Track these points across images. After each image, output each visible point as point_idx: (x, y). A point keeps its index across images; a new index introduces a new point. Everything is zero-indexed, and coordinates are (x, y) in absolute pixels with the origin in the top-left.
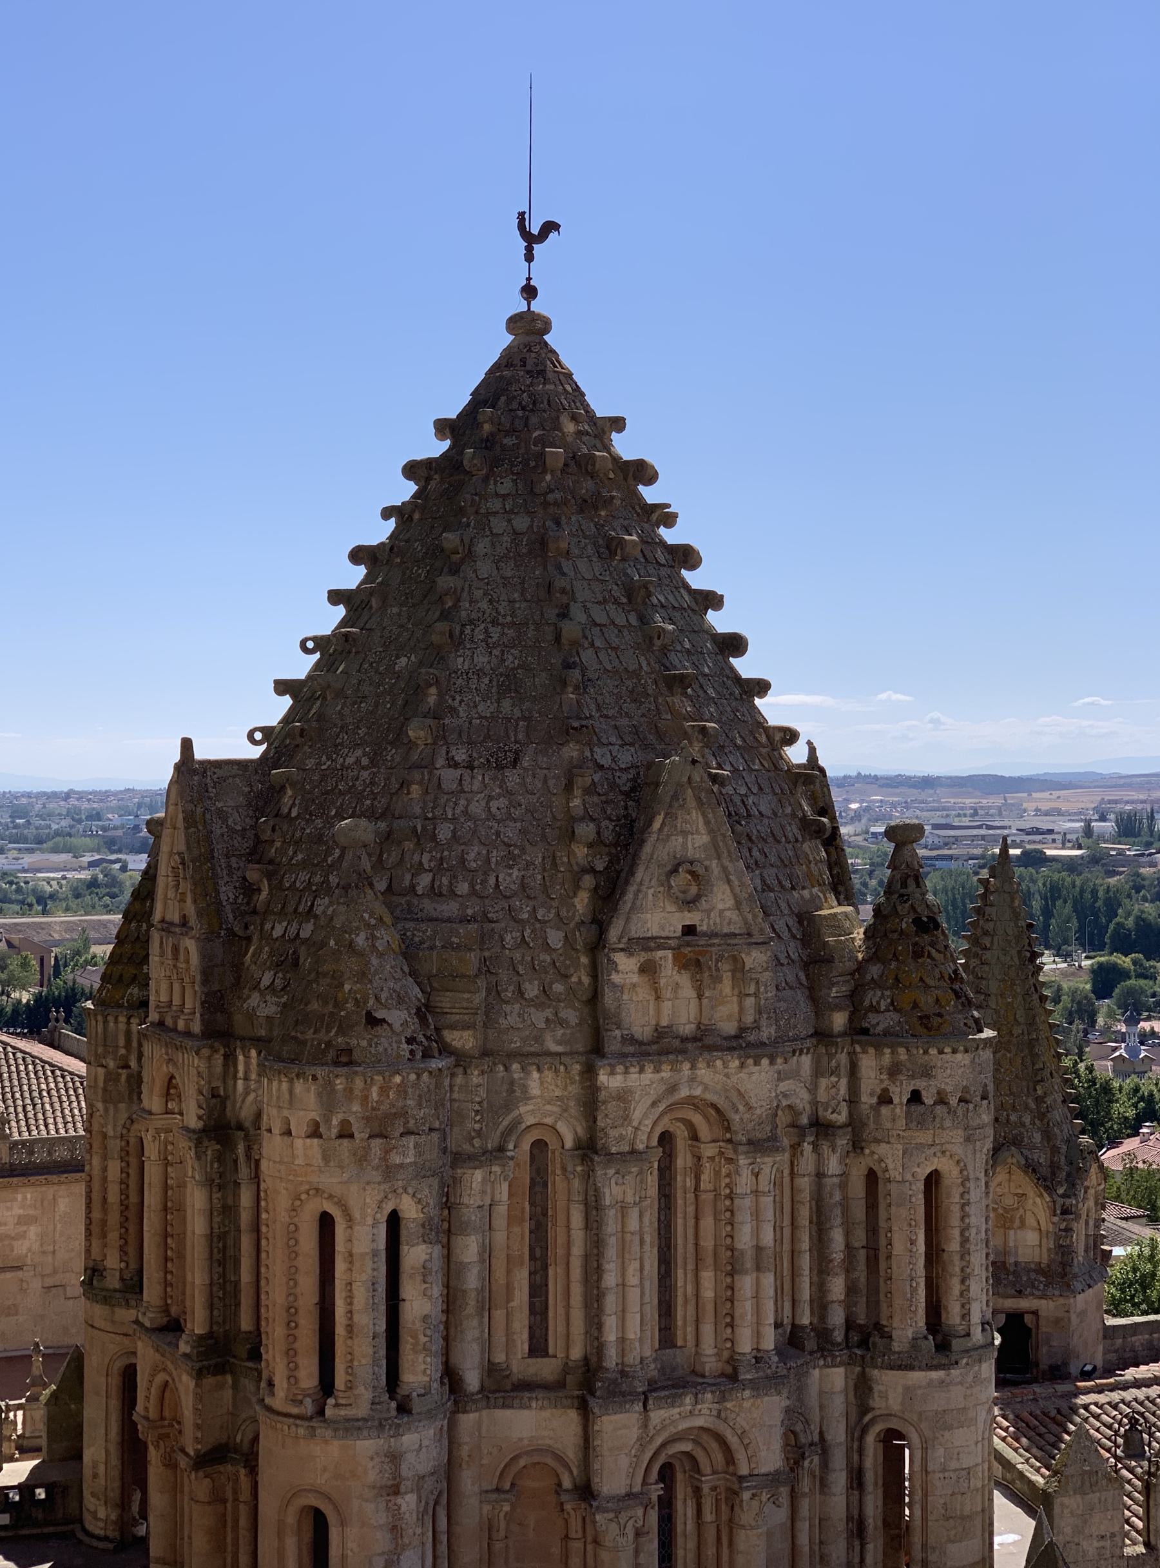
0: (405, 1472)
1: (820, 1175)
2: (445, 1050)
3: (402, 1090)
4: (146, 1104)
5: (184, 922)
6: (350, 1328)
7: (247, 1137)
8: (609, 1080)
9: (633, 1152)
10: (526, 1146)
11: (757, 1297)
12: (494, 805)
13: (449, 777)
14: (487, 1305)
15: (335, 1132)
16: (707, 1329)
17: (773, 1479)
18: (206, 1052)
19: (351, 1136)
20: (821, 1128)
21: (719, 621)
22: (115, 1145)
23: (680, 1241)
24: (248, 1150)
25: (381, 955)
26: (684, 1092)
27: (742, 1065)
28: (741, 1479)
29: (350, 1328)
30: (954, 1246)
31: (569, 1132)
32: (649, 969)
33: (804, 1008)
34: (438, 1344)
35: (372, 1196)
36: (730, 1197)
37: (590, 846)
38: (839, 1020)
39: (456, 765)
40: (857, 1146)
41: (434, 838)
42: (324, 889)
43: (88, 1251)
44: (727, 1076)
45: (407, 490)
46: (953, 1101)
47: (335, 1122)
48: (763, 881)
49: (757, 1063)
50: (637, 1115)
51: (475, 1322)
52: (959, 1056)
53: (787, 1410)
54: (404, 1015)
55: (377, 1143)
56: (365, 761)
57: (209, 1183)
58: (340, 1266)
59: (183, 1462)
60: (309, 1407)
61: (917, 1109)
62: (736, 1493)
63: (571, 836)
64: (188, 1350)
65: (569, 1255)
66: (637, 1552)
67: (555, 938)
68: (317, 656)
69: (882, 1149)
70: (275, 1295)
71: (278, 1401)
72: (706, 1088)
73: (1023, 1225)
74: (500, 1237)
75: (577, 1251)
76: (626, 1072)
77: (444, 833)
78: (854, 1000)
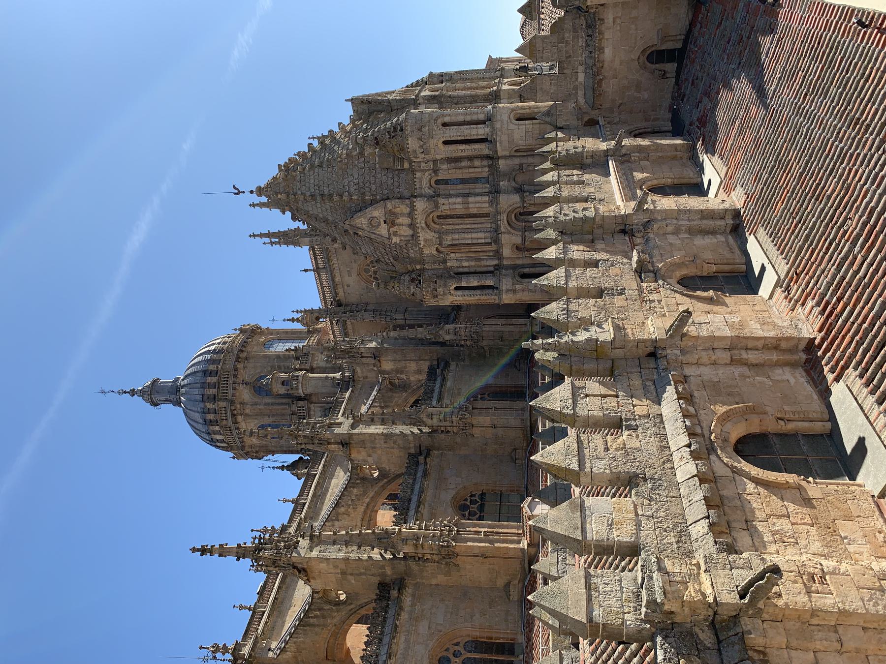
17: (522, 198)
26: (424, 225)
27: (416, 210)
30: (463, 138)
32: (395, 234)
35: (450, 297)
46: (422, 143)
52: (409, 142)
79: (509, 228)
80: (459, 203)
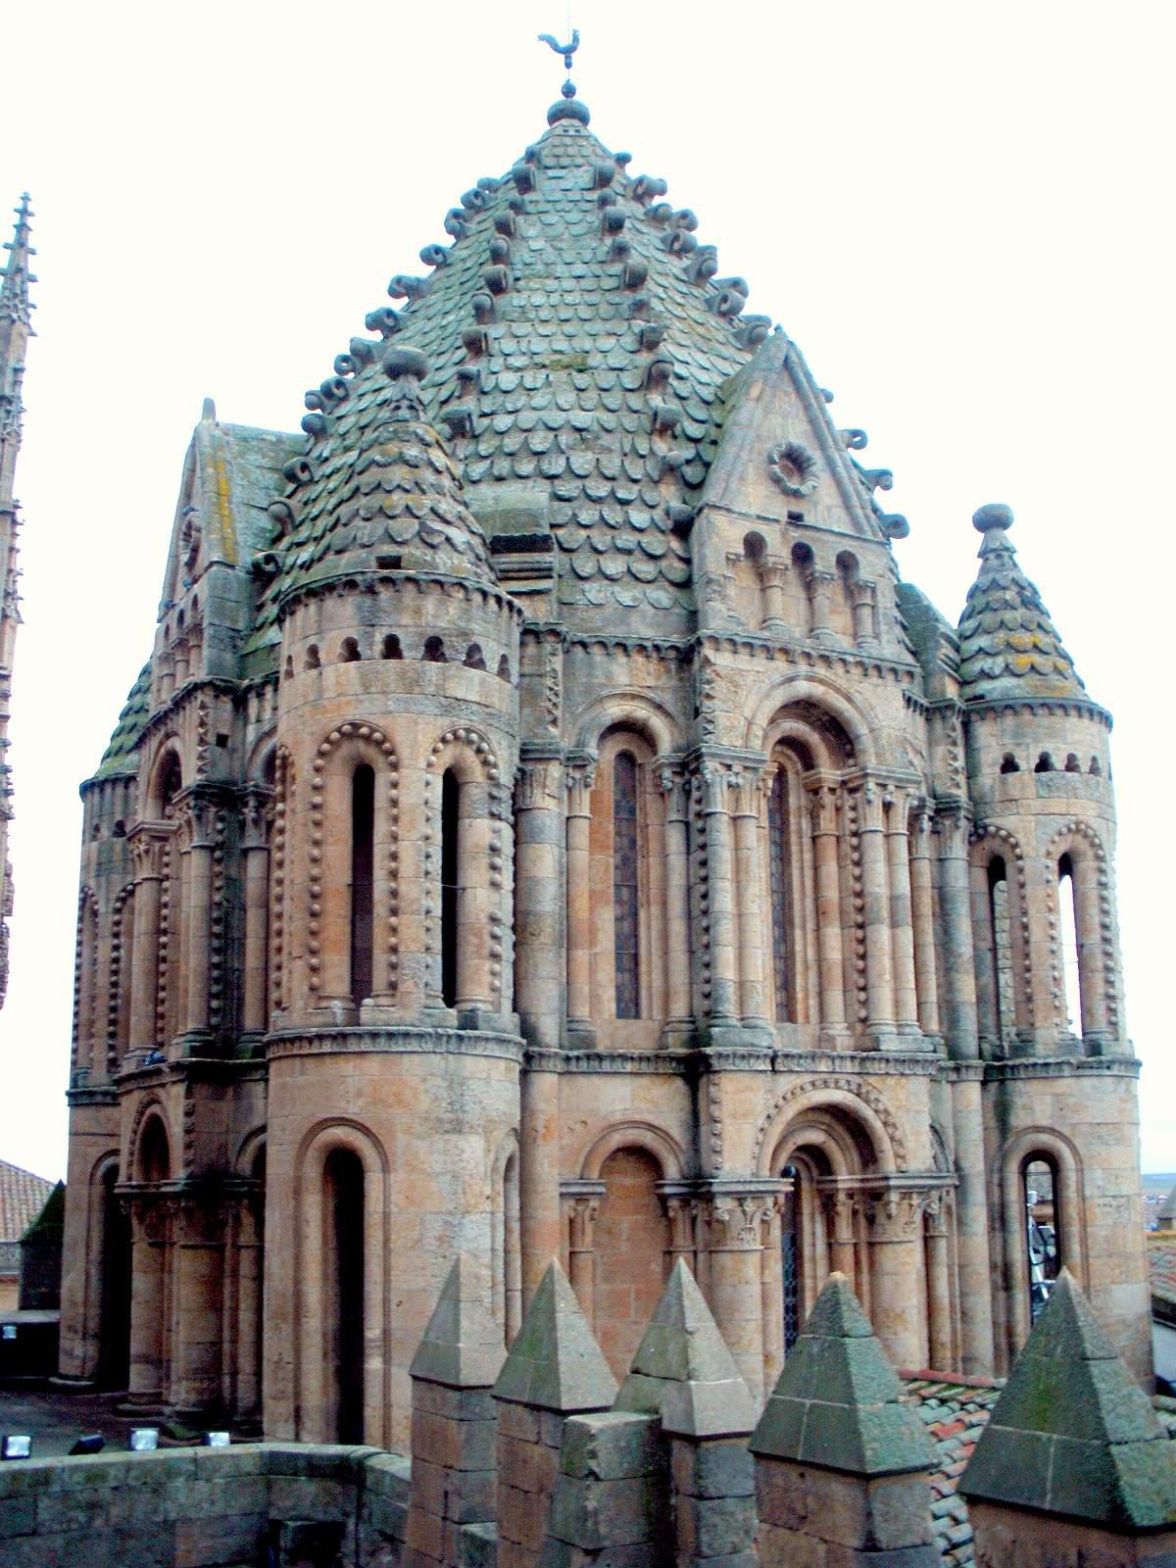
14: (568, 941)
15: (379, 647)
26: (803, 688)
32: (754, 545)
46: (1085, 766)
47: (379, 637)
58: (381, 828)
74: (582, 857)
75: (677, 881)
79: (790, 1111)
80: (892, 882)
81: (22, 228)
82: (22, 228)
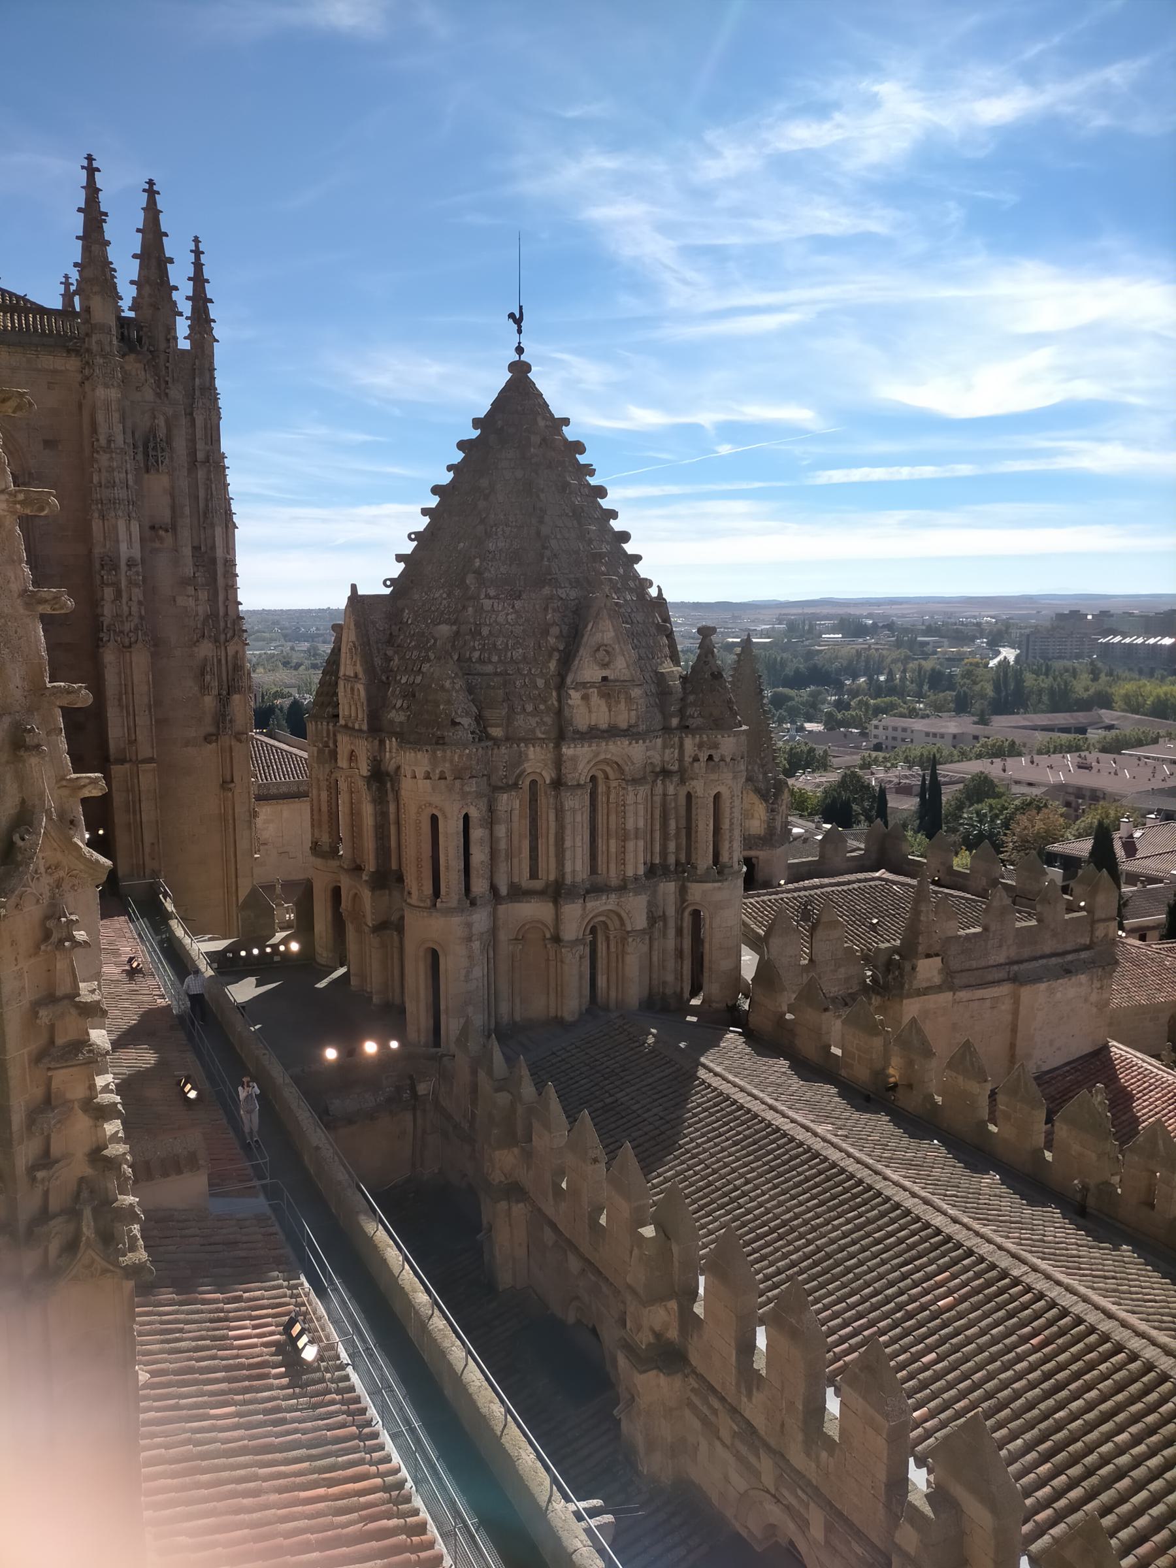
0: (474, 931)
1: (665, 795)
2: (489, 737)
3: (469, 756)
4: (340, 764)
5: (356, 676)
6: (447, 868)
7: (391, 780)
8: (568, 751)
9: (579, 785)
10: (527, 783)
11: (636, 851)
12: (510, 617)
13: (487, 603)
14: (510, 856)
15: (437, 776)
16: (613, 867)
17: (643, 931)
18: (370, 739)
19: (446, 778)
20: (665, 773)
21: (617, 525)
22: (324, 784)
23: (600, 826)
24: (392, 786)
25: (457, 692)
26: (602, 757)
27: (630, 743)
28: (628, 932)
29: (447, 868)
31: (548, 776)
32: (585, 698)
33: (659, 717)
34: (488, 875)
36: (624, 805)
37: (557, 638)
38: (675, 722)
39: (490, 598)
40: (683, 781)
41: (480, 633)
42: (427, 659)
43: (313, 835)
44: (623, 749)
45: (458, 457)
46: (728, 760)
47: (437, 772)
48: (640, 656)
49: (637, 743)
50: (580, 767)
51: (505, 864)
52: (731, 739)
53: (649, 902)
54: (469, 720)
55: (458, 782)
56: (445, 596)
57: (374, 801)
59: (366, 929)
60: (429, 903)
61: (712, 763)
62: (625, 939)
63: (548, 633)
64: (367, 878)
65: (548, 833)
66: (580, 966)
67: (540, 683)
68: (416, 543)
69: (694, 783)
70: (410, 853)
71: (414, 900)
72: (613, 754)
73: (753, 816)
74: (515, 825)
75: (552, 831)
76: (575, 747)
77: (485, 631)
78: (681, 713)
80: (636, 822)
81: (198, 266)
82: (198, 266)
